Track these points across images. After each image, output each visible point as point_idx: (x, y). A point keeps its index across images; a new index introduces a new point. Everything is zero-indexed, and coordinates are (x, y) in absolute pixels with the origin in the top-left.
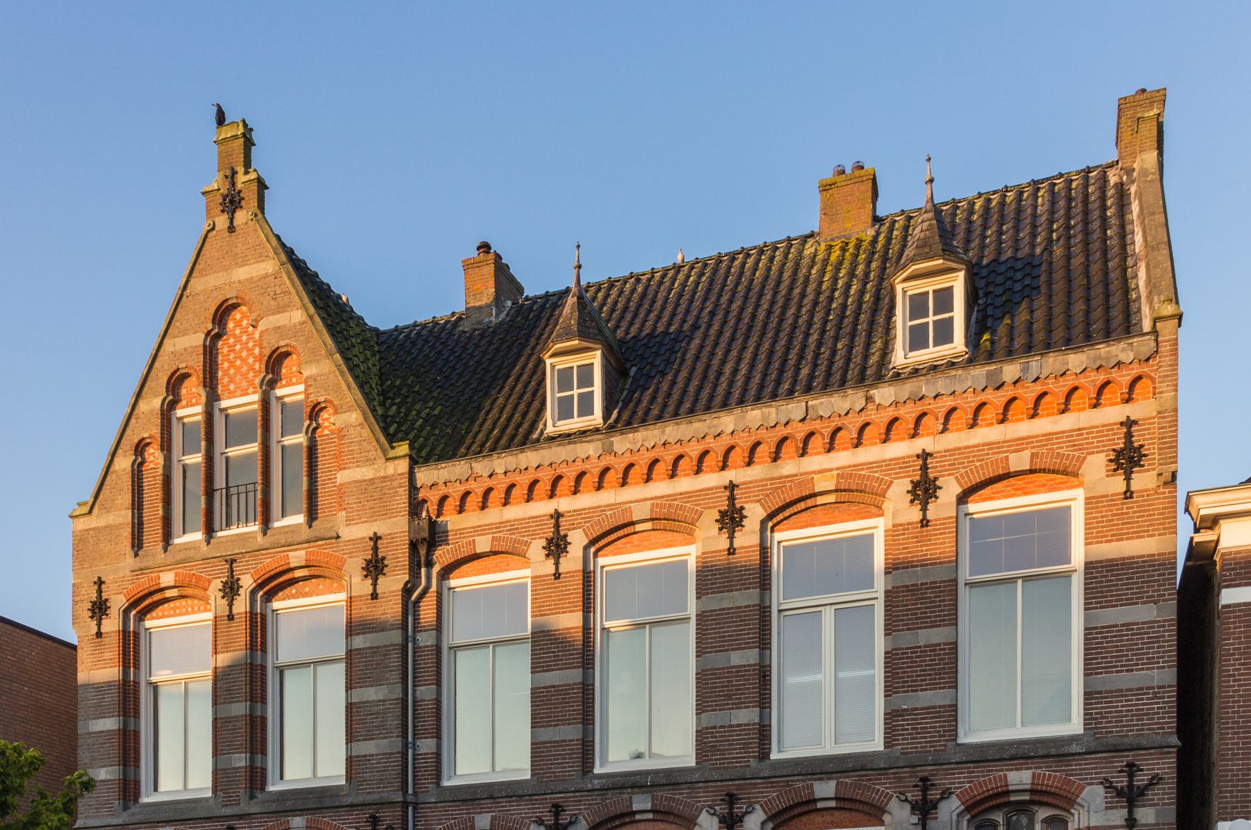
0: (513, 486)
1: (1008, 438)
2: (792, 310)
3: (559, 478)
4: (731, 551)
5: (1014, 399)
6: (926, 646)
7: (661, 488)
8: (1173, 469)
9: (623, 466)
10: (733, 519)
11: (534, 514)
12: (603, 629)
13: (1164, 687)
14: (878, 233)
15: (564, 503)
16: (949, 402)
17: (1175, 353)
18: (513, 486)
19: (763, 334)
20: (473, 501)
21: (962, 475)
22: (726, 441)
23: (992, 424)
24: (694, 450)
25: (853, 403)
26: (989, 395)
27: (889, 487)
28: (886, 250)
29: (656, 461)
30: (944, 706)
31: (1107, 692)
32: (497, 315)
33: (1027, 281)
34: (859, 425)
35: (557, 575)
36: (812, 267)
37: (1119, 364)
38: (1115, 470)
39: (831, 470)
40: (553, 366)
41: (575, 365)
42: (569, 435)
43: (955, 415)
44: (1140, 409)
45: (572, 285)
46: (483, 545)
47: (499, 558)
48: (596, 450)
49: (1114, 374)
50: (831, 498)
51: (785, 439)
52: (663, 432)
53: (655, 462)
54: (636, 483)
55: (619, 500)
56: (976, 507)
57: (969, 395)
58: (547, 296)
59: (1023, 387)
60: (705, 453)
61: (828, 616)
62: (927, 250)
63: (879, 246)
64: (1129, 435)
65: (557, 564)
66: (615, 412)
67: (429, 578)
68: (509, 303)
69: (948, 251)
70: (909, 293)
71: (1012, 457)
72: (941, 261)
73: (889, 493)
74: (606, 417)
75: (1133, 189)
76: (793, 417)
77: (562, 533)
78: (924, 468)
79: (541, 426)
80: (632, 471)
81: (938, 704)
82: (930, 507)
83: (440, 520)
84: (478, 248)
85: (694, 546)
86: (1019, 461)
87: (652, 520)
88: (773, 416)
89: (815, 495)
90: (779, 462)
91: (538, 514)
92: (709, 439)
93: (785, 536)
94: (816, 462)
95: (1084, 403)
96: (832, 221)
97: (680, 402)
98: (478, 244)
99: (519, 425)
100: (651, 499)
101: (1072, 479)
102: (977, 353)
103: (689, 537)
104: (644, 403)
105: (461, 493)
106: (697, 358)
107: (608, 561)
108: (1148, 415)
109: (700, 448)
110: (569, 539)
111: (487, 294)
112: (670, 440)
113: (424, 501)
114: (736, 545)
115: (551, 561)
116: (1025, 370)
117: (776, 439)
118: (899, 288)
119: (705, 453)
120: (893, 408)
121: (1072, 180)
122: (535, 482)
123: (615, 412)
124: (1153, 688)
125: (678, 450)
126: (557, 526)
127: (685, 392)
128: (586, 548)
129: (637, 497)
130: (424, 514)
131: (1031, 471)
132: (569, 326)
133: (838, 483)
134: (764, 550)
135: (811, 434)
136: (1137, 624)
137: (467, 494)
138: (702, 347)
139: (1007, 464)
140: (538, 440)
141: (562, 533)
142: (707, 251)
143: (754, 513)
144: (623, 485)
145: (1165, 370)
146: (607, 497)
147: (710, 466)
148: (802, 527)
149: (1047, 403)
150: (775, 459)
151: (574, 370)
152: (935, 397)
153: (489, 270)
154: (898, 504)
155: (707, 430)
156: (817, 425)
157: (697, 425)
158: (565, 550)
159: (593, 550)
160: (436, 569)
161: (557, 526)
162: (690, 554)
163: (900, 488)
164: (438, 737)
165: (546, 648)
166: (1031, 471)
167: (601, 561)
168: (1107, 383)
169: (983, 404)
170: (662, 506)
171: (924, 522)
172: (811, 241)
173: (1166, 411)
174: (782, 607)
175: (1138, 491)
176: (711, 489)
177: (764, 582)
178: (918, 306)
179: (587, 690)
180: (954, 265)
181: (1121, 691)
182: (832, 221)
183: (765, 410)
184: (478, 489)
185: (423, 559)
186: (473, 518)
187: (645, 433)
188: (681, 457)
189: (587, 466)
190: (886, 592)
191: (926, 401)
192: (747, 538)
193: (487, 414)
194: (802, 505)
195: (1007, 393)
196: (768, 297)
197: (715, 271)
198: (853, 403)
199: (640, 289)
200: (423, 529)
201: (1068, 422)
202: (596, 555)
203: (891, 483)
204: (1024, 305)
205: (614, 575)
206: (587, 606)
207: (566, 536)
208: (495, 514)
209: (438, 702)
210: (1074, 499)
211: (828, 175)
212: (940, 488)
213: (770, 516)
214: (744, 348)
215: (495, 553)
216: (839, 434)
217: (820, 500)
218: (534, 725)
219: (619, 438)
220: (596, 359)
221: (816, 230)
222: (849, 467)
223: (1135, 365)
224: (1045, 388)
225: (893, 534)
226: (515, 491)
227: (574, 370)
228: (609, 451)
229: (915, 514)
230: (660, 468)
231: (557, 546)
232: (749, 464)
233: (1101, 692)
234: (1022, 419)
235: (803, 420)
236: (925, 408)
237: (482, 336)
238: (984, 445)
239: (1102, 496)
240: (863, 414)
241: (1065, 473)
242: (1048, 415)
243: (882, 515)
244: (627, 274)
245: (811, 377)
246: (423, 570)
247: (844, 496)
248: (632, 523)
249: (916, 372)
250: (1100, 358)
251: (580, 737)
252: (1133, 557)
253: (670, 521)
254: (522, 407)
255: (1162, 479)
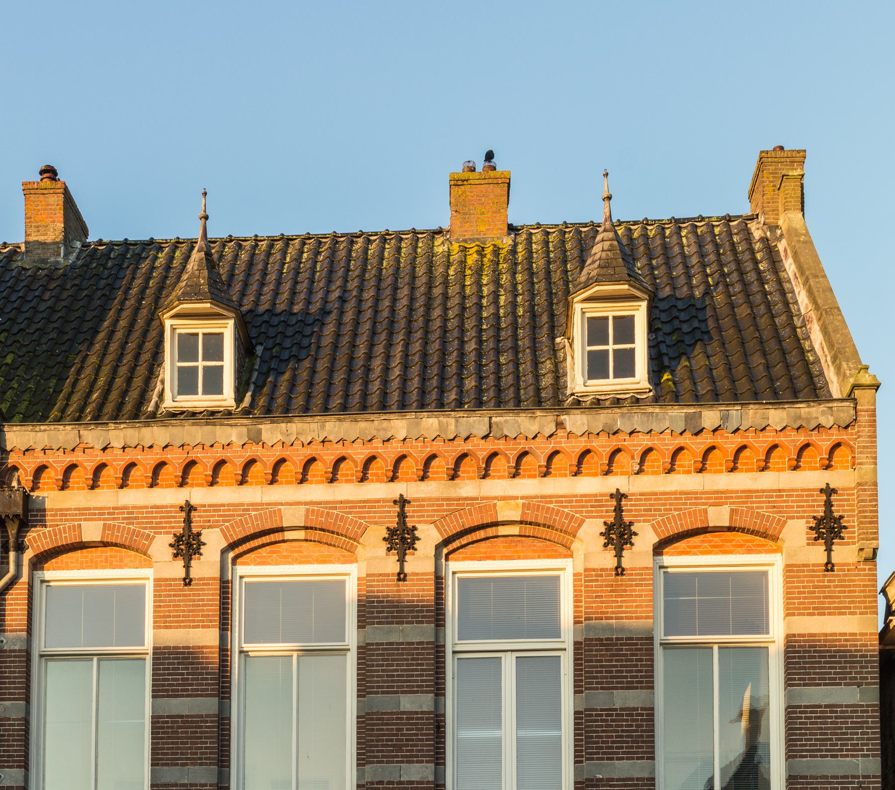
0: (132, 465)
1: (707, 489)
2: (437, 313)
3: (192, 463)
4: (402, 576)
5: (712, 448)
6: (622, 709)
7: (316, 491)
8: (874, 546)
9: (273, 460)
10: (403, 539)
11: (159, 502)
12: (241, 652)
13: (868, 777)
14: (515, 245)
15: (198, 495)
16: (644, 441)
17: (873, 424)
18: (132, 465)
19: (409, 332)
20: (80, 477)
21: (658, 523)
22: (396, 448)
23: (689, 472)
24: (359, 454)
25: (542, 426)
26: (687, 440)
27: (580, 526)
28: (556, 261)
29: (312, 460)
30: (642, 779)
31: (812, 777)
32: (66, 255)
33: (696, 324)
34: (548, 451)
35: (187, 581)
36: (448, 267)
37: (819, 427)
38: (816, 539)
39: (516, 498)
40: (173, 329)
41: (201, 331)
42: (194, 414)
43: (651, 456)
44: (838, 478)
45: (197, 234)
46: (91, 532)
47: (109, 552)
48: (240, 436)
49: (814, 437)
50: (515, 530)
51: (464, 456)
52: (323, 427)
53: (312, 460)
54: (287, 483)
55: (266, 500)
56: (673, 560)
57: (667, 436)
58: (126, 243)
59: (722, 436)
60: (371, 459)
61: (509, 665)
62: (611, 271)
63: (520, 257)
64: (828, 504)
65: (187, 567)
66: (249, 394)
67: (19, 565)
68: (78, 244)
69: (632, 277)
70: (588, 315)
71: (711, 510)
72: (626, 287)
73: (581, 533)
74: (239, 399)
75: (781, 246)
76: (474, 432)
77: (195, 530)
78: (619, 510)
79: (155, 398)
80: (283, 468)
81: (636, 776)
82: (624, 553)
83: (35, 494)
84: (41, 173)
85: (355, 565)
86: (719, 516)
87: (306, 528)
88: (452, 427)
89: (496, 524)
90: (457, 481)
91: (164, 503)
92: (377, 443)
93: (460, 567)
94: (497, 487)
95: (784, 463)
96: (464, 221)
97: (328, 396)
98: (42, 166)
99: (124, 393)
100: (306, 503)
101: (771, 543)
102: (663, 394)
103: (350, 555)
104: (283, 389)
105: (64, 465)
106: (335, 346)
107: (250, 571)
108: (847, 485)
109: (367, 452)
110: (203, 539)
111: (53, 230)
112: (331, 438)
113: (15, 468)
114: (407, 569)
115: (180, 563)
116: (725, 418)
117: (455, 455)
118: (578, 307)
119: (371, 459)
120: (584, 438)
121: (713, 226)
122: (161, 464)
123: (249, 394)
124: (858, 777)
125: (340, 451)
126: (188, 521)
127: (330, 384)
128: (224, 552)
129: (291, 500)
130: (14, 484)
131: (730, 529)
132: (198, 285)
133: (523, 514)
134: (439, 581)
135: (494, 454)
136: (841, 706)
137: (72, 467)
138: (338, 335)
139: (706, 518)
140: (153, 415)
141: (195, 530)
142: (322, 227)
143: (429, 536)
144: (272, 482)
145: (864, 440)
146: (252, 494)
147: (376, 475)
148: (480, 559)
149: (747, 458)
150: (453, 477)
151: (198, 338)
152: (631, 434)
153: (57, 200)
154: (590, 546)
155: (374, 433)
156: (501, 445)
157: (363, 425)
158: (197, 552)
159: (231, 555)
160: (28, 555)
161: (188, 521)
162: (353, 574)
163: (592, 530)
164: (26, 767)
165: (175, 670)
166: (730, 529)
167: (241, 570)
168: (807, 446)
169: (681, 449)
170: (319, 514)
171: (619, 570)
172: (439, 240)
173: (866, 484)
174: (458, 648)
175: (839, 565)
176: (378, 501)
177: (438, 615)
178: (596, 330)
179: (222, 723)
180: (638, 293)
181: (826, 777)
182: (464, 221)
183: (444, 420)
184: (88, 463)
185: (12, 540)
186: (77, 498)
187: (300, 425)
188: (342, 459)
189: (227, 454)
190: (575, 643)
191: (620, 436)
192: (420, 562)
193: (79, 372)
194: (481, 534)
195: (706, 440)
196: (404, 292)
197: (333, 250)
198: (542, 426)
199: (244, 256)
200: (16, 504)
201: (767, 481)
202: (234, 562)
203: (583, 521)
204: (698, 348)
205: (253, 588)
206: (225, 624)
207: (199, 534)
208: (107, 497)
209: (26, 722)
210: (773, 566)
211: (458, 169)
212: (635, 534)
213: (446, 542)
214: (390, 345)
215: (105, 544)
216: (525, 459)
217: (502, 530)
218: (155, 762)
219: (269, 426)
220: (227, 329)
221: (446, 226)
222: (536, 497)
223: (834, 431)
224: (745, 441)
225: (587, 579)
226: (255, 469)
227: (198, 338)
228: (256, 438)
229: (608, 560)
230: (317, 469)
231: (187, 546)
232: (423, 478)
233: (806, 777)
234: (721, 471)
235: (485, 437)
236: (620, 444)
237: (50, 277)
238: (682, 493)
239: (804, 565)
240: (552, 440)
241: (764, 535)
242: (748, 470)
243: (571, 556)
244: (225, 236)
245: (479, 390)
246: (12, 555)
247: (529, 530)
248: (281, 530)
249: (598, 404)
250: (800, 417)
251: (215, 781)
252: (835, 634)
253: (328, 533)
254: (123, 370)
255: (864, 555)
